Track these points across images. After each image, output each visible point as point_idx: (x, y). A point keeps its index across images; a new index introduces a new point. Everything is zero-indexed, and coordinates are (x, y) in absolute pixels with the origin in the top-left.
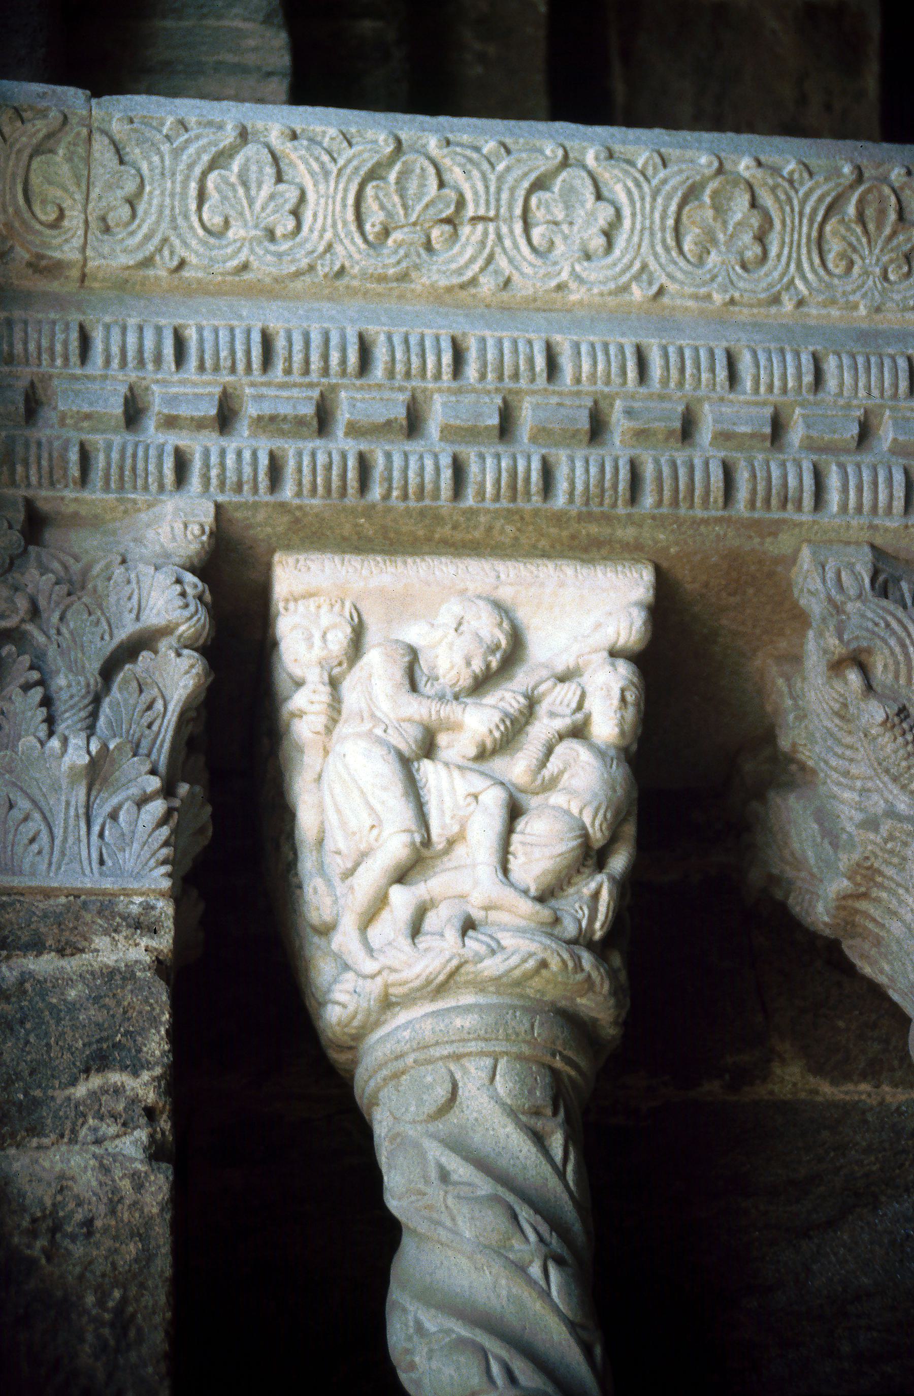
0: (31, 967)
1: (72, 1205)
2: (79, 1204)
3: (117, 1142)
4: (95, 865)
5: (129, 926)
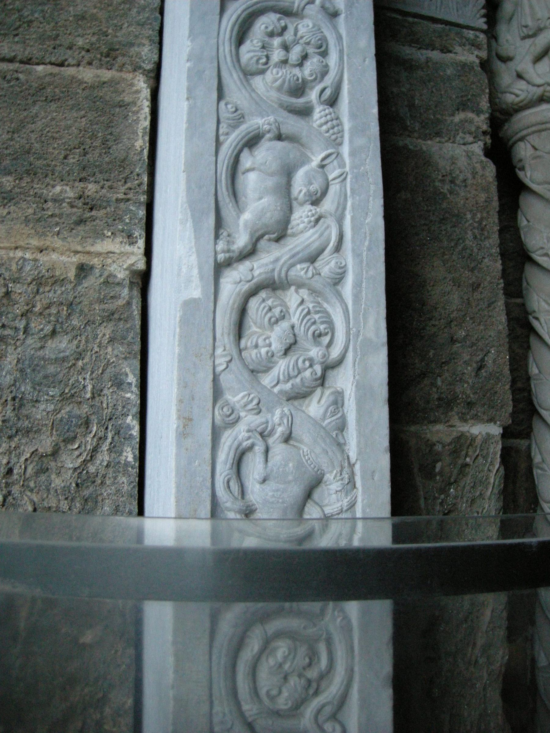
0: (430, 55)
1: (458, 172)
2: (460, 172)
3: (472, 145)
4: (455, 10)
5: (469, 44)
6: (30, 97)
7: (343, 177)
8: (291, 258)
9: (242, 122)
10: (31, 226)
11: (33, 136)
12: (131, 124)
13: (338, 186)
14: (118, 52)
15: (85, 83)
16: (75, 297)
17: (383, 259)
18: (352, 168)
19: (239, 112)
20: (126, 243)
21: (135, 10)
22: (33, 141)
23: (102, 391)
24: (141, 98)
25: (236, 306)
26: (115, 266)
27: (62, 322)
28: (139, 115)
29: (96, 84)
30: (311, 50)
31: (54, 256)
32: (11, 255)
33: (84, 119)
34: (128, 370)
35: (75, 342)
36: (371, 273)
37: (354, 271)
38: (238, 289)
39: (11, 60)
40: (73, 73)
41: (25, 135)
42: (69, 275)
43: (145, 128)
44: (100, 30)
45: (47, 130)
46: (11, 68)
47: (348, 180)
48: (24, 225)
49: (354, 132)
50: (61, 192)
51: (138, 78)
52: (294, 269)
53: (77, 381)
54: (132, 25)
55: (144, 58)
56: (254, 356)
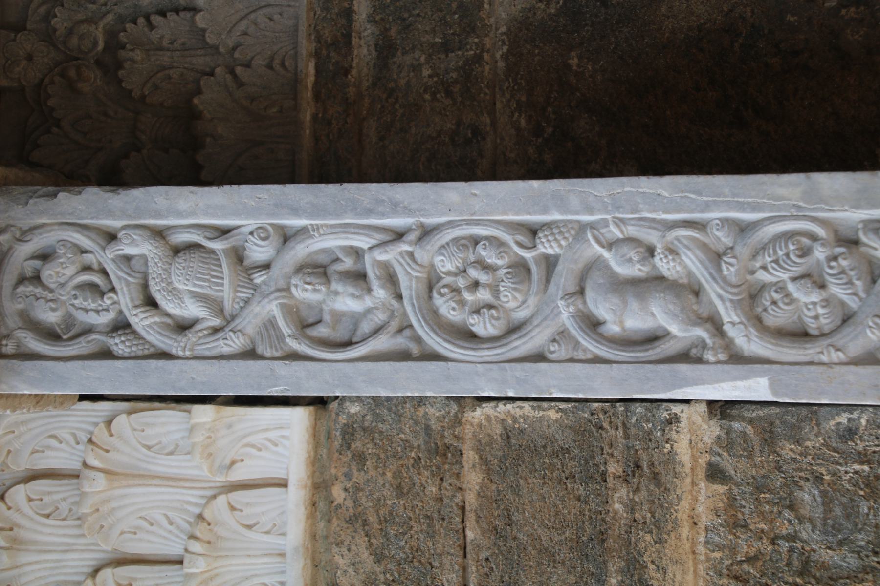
6: (508, 545)
7: (620, 222)
8: (716, 282)
9: (569, 333)
10: (666, 536)
11: (557, 538)
12: (529, 425)
13: (630, 228)
14: (439, 444)
15: (483, 480)
16: (748, 484)
17: (709, 178)
18: (607, 212)
19: (557, 338)
20: (678, 427)
21: (380, 425)
22: (563, 538)
23: (859, 453)
24: (496, 414)
25: (774, 341)
26: (706, 438)
27: (779, 498)
28: (517, 416)
29: (483, 467)
30: (472, 258)
31: (700, 509)
32: (703, 557)
33: (530, 481)
34: (832, 423)
35: (802, 483)
36: (727, 191)
37: (726, 211)
38: (755, 339)
39: (464, 569)
40: (472, 495)
41: (557, 548)
42: (721, 492)
43: (533, 408)
44: (413, 466)
45: (546, 522)
46: (474, 568)
47: (621, 216)
48: (665, 545)
49: (564, 208)
50: (621, 503)
51: (470, 419)
52: (729, 278)
53: (849, 481)
54: (401, 428)
55: (443, 412)
56: (827, 321)
